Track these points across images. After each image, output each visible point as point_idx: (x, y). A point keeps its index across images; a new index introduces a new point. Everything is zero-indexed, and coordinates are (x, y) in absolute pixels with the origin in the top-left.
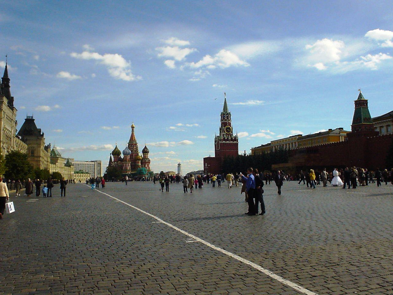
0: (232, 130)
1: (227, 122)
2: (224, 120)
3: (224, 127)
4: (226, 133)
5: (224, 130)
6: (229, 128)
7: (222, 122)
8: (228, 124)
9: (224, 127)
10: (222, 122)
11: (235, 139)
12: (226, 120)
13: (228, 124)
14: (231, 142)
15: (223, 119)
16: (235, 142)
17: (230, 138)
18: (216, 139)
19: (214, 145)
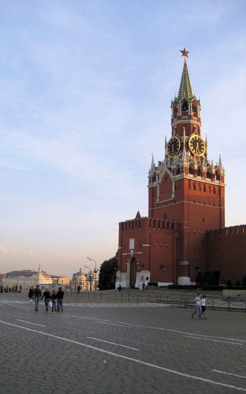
0: (206, 148)
1: (193, 125)
2: (187, 117)
3: (186, 135)
4: (192, 154)
5: (187, 143)
6: (200, 141)
7: (179, 122)
8: (196, 130)
9: (186, 135)
10: (179, 122)
11: (216, 172)
12: (190, 117)
14: (208, 181)
15: (183, 114)
16: (216, 182)
17: (205, 169)
18: (158, 172)
19: (147, 190)
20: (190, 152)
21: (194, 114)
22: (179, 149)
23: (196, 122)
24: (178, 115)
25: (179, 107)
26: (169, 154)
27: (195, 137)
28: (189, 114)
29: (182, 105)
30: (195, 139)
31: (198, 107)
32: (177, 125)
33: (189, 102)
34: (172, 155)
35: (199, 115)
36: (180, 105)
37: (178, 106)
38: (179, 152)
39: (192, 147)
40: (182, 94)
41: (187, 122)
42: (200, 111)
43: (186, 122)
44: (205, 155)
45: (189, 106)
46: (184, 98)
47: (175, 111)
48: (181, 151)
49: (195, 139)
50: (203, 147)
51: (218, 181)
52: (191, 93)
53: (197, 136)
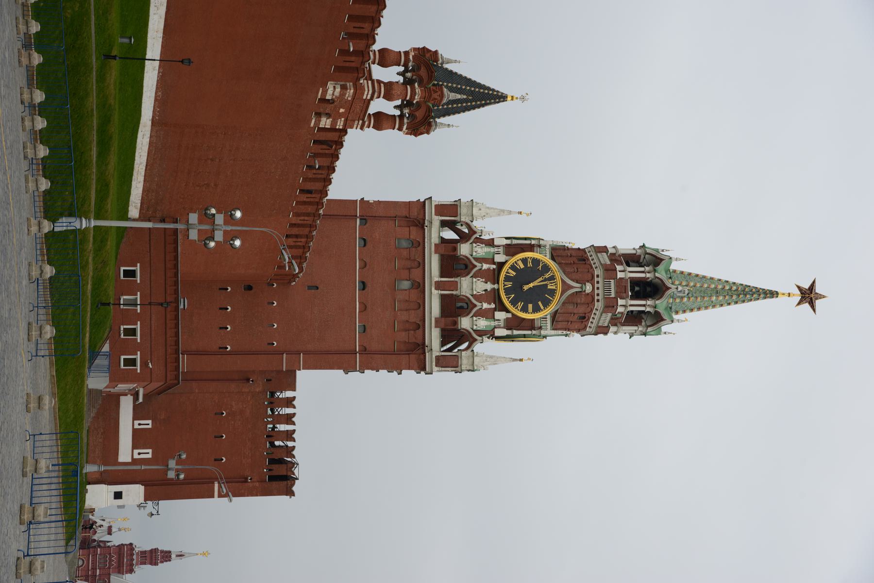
7: (599, 305)
10: (599, 305)
24: (621, 302)
25: (644, 306)
26: (513, 267)
28: (613, 329)
32: (591, 296)
33: (649, 329)
34: (507, 278)
36: (648, 309)
37: (649, 302)
38: (508, 311)
40: (682, 298)
45: (636, 328)
46: (663, 320)
48: (509, 315)
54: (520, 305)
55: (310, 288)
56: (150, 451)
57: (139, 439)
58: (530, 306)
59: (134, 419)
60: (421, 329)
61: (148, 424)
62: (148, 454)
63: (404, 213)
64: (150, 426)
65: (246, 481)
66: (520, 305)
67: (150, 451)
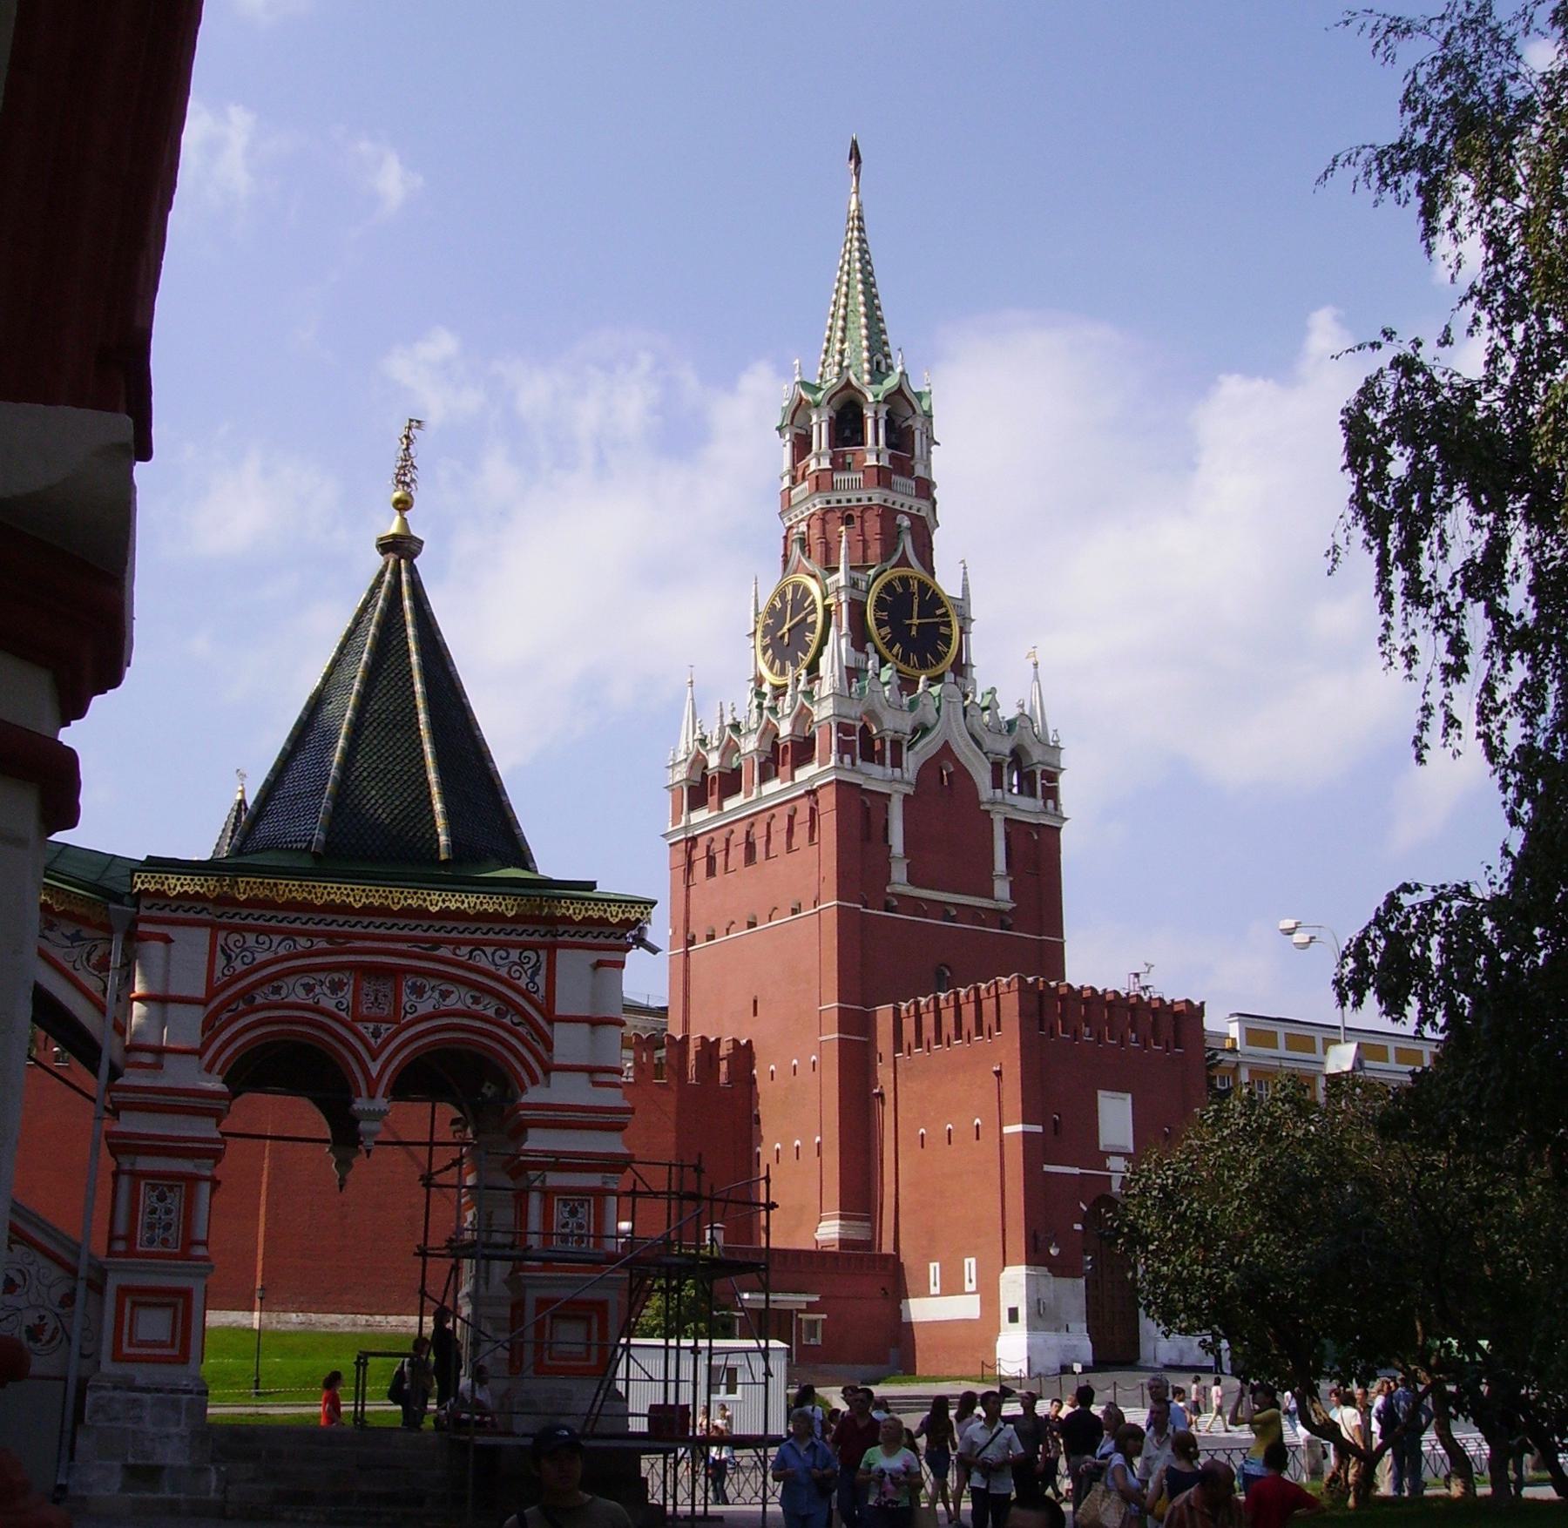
13: (907, 543)
15: (839, 464)
20: (877, 651)
21: (892, 457)
22: (813, 638)
23: (908, 501)
24: (813, 466)
26: (771, 668)
27: (904, 581)
29: (833, 414)
30: (900, 590)
31: (919, 425)
33: (871, 399)
35: (928, 466)
36: (825, 417)
37: (814, 419)
39: (887, 630)
41: (859, 500)
42: (934, 448)
43: (854, 503)
44: (961, 668)
45: (870, 424)
47: (802, 446)
49: (900, 590)
50: (943, 630)
51: (1025, 803)
52: (887, 356)
53: (917, 570)
54: (809, 637)
55: (755, 1014)
56: (967, 1261)
57: (952, 1286)
58: (810, 620)
59: (925, 1293)
60: (797, 803)
61: (934, 1267)
62: (970, 1264)
63: (680, 872)
64: (937, 1264)
65: (998, 1074)
66: (809, 637)
67: (967, 1261)
